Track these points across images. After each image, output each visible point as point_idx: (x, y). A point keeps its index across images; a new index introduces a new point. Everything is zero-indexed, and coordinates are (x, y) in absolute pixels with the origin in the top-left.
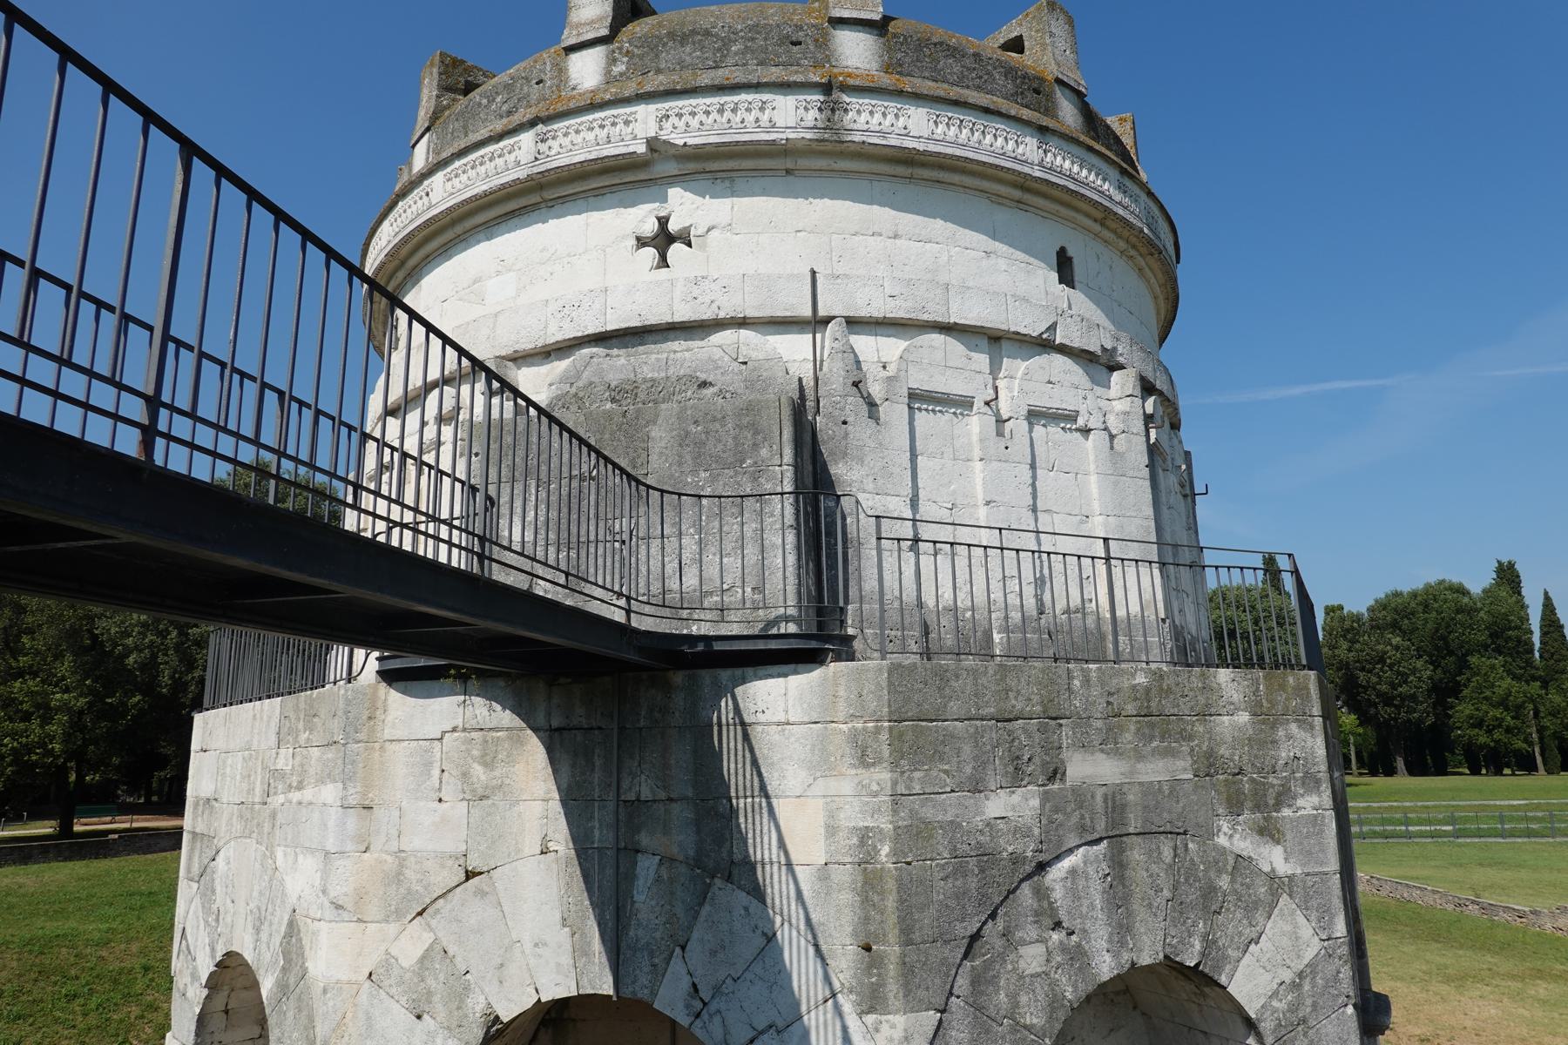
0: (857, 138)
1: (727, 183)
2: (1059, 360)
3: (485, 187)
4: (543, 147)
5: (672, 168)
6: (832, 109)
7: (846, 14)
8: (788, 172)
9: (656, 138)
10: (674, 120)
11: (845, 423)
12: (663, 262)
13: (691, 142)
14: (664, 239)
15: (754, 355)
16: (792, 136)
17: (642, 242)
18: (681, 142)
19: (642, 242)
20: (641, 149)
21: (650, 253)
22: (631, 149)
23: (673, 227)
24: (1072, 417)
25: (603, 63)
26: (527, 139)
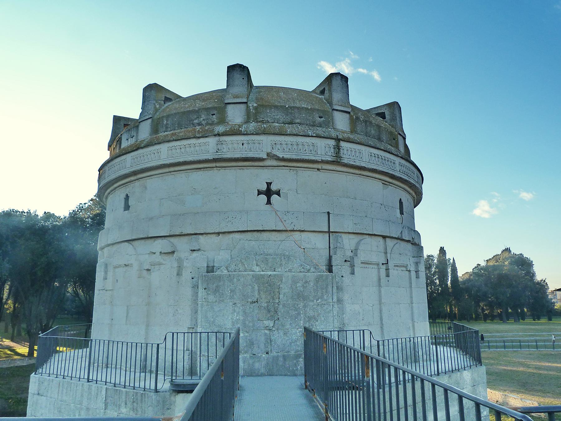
1: (295, 172)
2: (403, 244)
4: (219, 147)
5: (275, 163)
6: (338, 148)
10: (278, 146)
11: (342, 277)
12: (269, 202)
13: (286, 157)
14: (269, 193)
15: (308, 246)
17: (260, 193)
18: (281, 156)
19: (260, 193)
20: (265, 156)
21: (264, 198)
23: (274, 188)
24: (406, 267)
26: (212, 141)
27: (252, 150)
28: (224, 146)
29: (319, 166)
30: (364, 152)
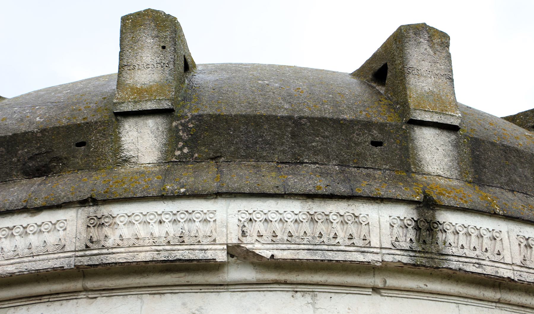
0: (454, 264)
3: (11, 269)
4: (95, 233)
6: (426, 230)
7: (427, 118)
8: (376, 290)
9: (238, 246)
10: (260, 227)
13: (279, 255)
16: (388, 259)
18: (267, 254)
20: (222, 257)
22: (209, 255)
25: (162, 139)
27: (186, 240)
28: (106, 230)
29: (378, 281)
30: (504, 236)
